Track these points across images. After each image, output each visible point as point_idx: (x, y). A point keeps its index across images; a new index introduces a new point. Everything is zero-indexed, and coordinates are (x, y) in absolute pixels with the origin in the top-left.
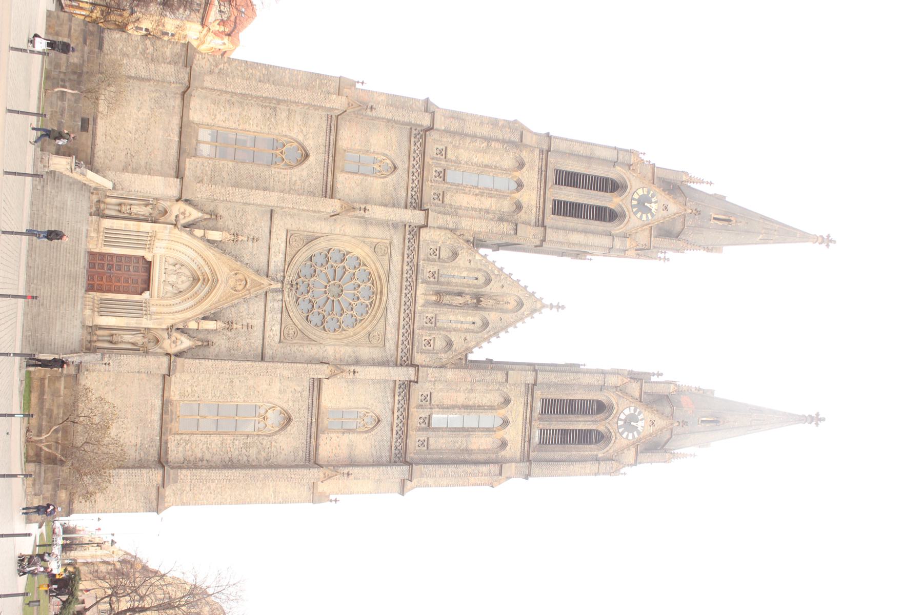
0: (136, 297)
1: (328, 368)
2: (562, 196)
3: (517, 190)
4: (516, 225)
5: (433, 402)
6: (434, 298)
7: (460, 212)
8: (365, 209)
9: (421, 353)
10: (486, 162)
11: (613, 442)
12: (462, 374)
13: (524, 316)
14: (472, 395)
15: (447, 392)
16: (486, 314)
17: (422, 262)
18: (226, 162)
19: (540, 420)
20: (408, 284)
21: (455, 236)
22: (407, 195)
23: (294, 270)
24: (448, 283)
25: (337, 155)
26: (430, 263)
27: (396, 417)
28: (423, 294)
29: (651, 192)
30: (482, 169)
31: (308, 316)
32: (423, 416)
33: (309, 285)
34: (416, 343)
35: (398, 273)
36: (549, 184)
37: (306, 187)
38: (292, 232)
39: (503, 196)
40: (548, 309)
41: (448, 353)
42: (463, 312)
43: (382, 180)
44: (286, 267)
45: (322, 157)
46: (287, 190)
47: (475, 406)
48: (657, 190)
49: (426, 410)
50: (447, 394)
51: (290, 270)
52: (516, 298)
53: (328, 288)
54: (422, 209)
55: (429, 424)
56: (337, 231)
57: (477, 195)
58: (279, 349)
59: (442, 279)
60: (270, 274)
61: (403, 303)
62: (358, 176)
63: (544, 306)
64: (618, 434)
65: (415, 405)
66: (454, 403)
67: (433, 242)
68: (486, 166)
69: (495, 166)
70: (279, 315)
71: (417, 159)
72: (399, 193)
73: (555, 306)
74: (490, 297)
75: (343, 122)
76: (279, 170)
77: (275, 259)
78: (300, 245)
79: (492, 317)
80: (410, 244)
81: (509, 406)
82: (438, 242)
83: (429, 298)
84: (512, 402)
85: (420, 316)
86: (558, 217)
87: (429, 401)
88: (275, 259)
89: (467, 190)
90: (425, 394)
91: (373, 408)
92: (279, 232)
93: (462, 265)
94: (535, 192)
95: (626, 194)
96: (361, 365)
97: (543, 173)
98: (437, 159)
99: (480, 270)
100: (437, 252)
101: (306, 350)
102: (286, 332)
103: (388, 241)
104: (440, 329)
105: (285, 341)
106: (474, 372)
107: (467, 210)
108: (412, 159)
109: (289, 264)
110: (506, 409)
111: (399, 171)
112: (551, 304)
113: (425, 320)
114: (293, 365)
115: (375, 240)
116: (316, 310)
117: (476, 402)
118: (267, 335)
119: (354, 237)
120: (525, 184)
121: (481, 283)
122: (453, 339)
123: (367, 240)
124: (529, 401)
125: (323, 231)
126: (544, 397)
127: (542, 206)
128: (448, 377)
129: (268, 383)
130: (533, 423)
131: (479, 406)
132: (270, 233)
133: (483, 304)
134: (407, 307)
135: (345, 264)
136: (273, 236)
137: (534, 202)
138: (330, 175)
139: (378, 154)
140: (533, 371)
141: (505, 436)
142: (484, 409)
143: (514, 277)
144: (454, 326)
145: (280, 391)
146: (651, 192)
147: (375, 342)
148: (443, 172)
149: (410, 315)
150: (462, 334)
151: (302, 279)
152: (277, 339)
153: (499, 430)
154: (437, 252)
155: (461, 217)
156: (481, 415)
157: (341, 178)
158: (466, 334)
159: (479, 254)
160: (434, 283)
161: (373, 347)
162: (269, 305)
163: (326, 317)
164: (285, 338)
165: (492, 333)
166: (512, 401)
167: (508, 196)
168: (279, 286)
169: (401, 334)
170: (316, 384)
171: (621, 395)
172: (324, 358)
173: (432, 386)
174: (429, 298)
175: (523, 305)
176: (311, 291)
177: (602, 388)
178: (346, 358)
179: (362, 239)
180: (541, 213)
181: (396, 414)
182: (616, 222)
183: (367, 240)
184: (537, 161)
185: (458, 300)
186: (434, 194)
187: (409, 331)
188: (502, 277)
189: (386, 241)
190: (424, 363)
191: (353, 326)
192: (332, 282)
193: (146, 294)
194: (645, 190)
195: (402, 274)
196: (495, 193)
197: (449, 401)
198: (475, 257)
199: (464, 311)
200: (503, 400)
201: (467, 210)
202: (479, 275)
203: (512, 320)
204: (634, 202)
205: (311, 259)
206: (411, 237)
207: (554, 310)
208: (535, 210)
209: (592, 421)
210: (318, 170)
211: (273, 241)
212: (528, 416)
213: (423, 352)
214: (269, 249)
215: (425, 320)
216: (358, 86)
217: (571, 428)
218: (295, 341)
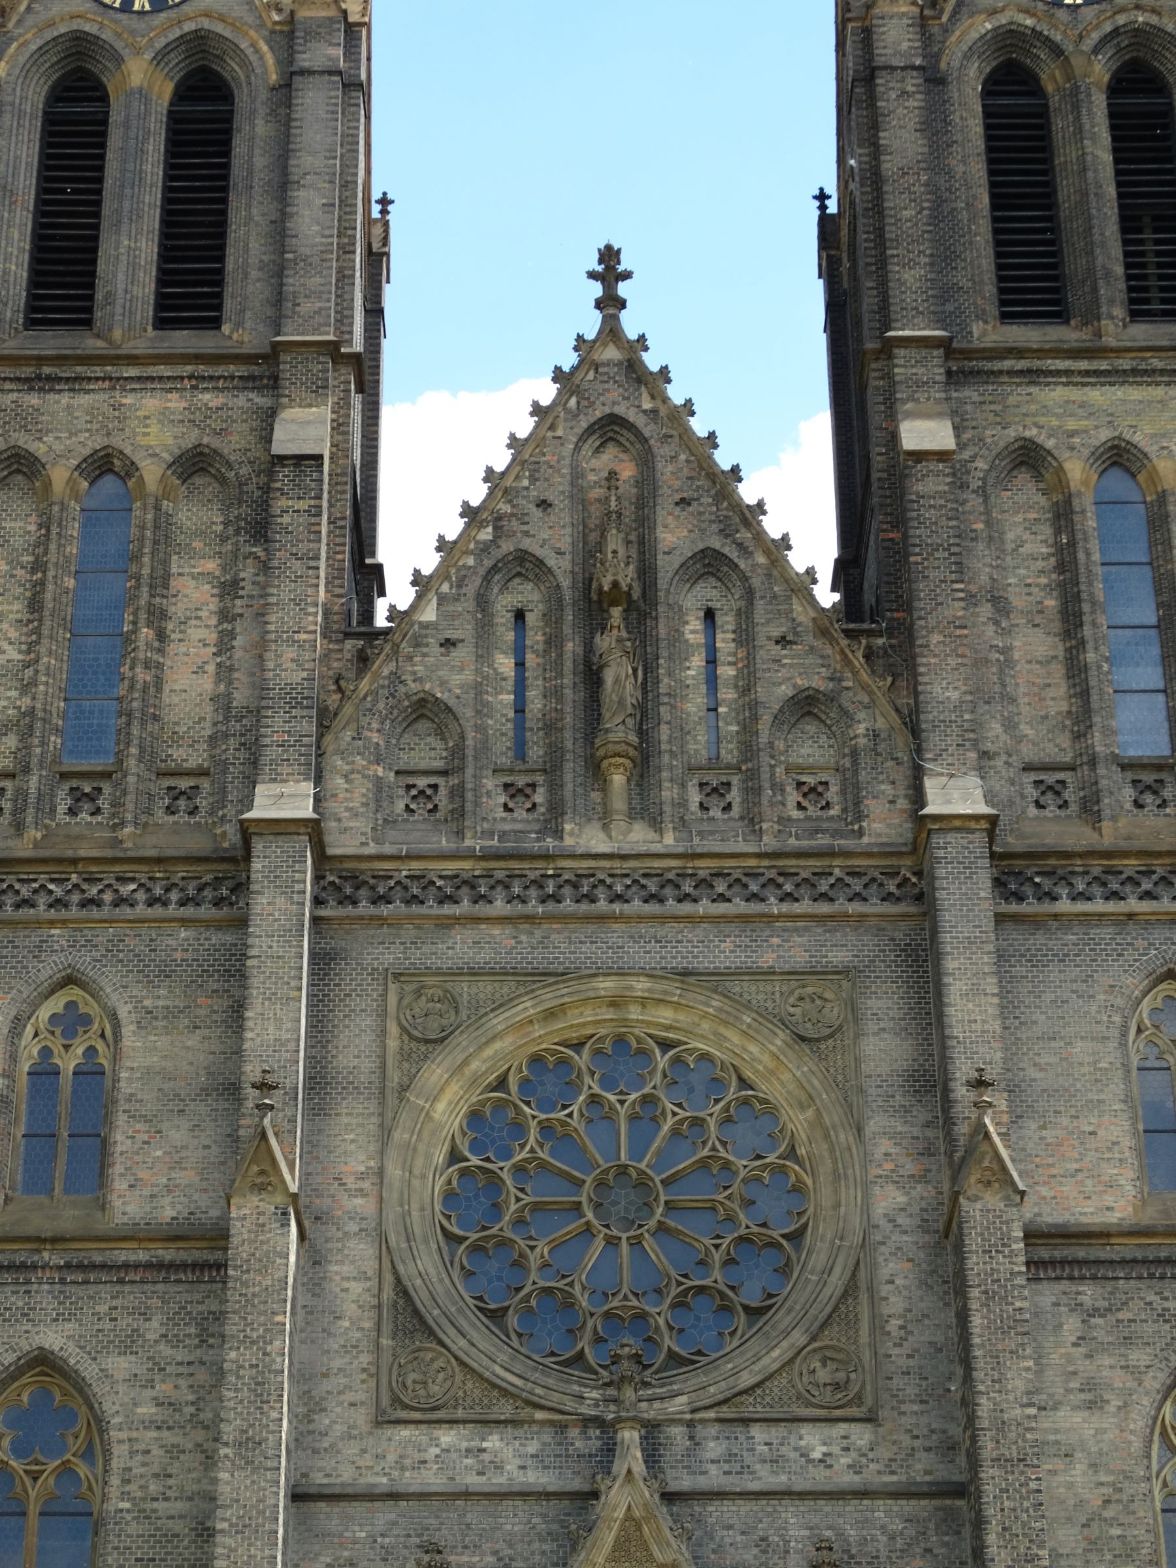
1: (976, 1198)
2: (137, 291)
3: (129, 475)
4: (282, 459)
5: (1067, 758)
6: (618, 780)
7: (240, 697)
8: (264, 1087)
9: (859, 817)
10: (16, 607)
11: (1154, 20)
12: (936, 638)
13: (663, 411)
14: (1018, 601)
15: (1013, 700)
16: (666, 566)
17: (468, 843)
19: (1092, 316)
20: (567, 891)
21: (348, 710)
22: (184, 922)
23: (551, 1382)
24: (551, 726)
25: (30, 1231)
26: (469, 807)
27: (1146, 906)
28: (606, 827)
30: (48, 623)
31: (746, 1308)
32: (1128, 793)
33: (608, 1315)
34: (822, 841)
35: (523, 938)
36: (92, 344)
37: (181, 1355)
38: (385, 1401)
39: (156, 527)
40: (624, 315)
41: (846, 704)
42: (670, 658)
43: (128, 1030)
44: (539, 1415)
45: (44, 1297)
46: (199, 1435)
47: (1062, 586)
49: (1104, 783)
50: (1023, 700)
51: (556, 1397)
52: (587, 449)
53: (615, 1232)
54: (240, 853)
55: (1159, 767)
56: (364, 1205)
57: (162, 636)
58: (906, 1421)
59: (535, 752)
60: (577, 1484)
61: (653, 908)
62: (121, 1141)
63: (611, 330)
65: (1087, 830)
66: (1058, 671)
67: (378, 801)
68: (35, 605)
69: (33, 571)
70: (758, 1433)
71: (25, 892)
72: (178, 955)
76: (115, 1481)
78: (440, 1363)
80: (398, 894)
81: (1050, 444)
82: (378, 782)
83: (619, 802)
84: (1031, 433)
85: (700, 833)
86: (229, 305)
87: (1061, 776)
89: (142, 675)
90: (1032, 793)
91: (1120, 1002)
92: (391, 1458)
93: (468, 676)
94: (128, 400)
95: (107, 35)
96: (945, 1059)
97: (47, 370)
98: (19, 811)
99: (483, 603)
100: (422, 782)
101: (895, 1304)
102: (828, 1397)
103: (393, 987)
104: (748, 750)
105: (869, 1401)
106: (922, 589)
107: (231, 669)
108: (26, 912)
109: (529, 1403)
110: (1064, 455)
111: (84, 961)
112: (599, 304)
113: (715, 812)
114: (978, 1353)
115: (393, 1044)
116: (716, 1276)
117: (1044, 580)
118: (848, 1480)
119: (385, 1133)
120: (98, 442)
121: (536, 596)
122: (785, 691)
123: (395, 1078)
124: (1021, 365)
125: (370, 1266)
126: (993, 310)
127: (189, 369)
128: (954, 695)
129: (1059, 1464)
130: (1110, 341)
131: (1061, 568)
132: (393, 1496)
133: (627, 576)
134: (668, 891)
135: (504, 1169)
136: (411, 1481)
137: (176, 403)
138: (122, 1257)
139: (13, 1058)
140: (890, 357)
142: (1072, 544)
143: (501, 460)
144: (727, 694)
145: (1090, 1406)
147: (834, 1013)
148: (74, 783)
149: (702, 874)
150: (761, 654)
151: (584, 1343)
152: (861, 1435)
153: (1154, 477)
154: (422, 782)
155: (261, 688)
156: (1096, 557)
158: (761, 640)
159: (414, 607)
160: (555, 787)
161: (856, 1021)
162: (714, 1478)
163: (743, 1231)
164: (858, 1400)
165: (744, 535)
166: (1027, 434)
167: (157, 508)
168: (630, 1436)
169: (785, 908)
170: (1044, 1254)
172: (924, 1226)
173: (999, 762)
174: (619, 802)
176: (635, 1303)
178: (916, 1131)
179: (392, 1100)
180: (220, 370)
181: (1133, 904)
182: (232, 69)
183: (395, 1078)
185: (617, 681)
186: (170, 810)
187: (772, 874)
188: (506, 508)
189: (392, 999)
190: (903, 804)
191: (770, 1110)
192: (590, 1215)
195: (529, 919)
196: (146, 559)
197: (1051, 693)
198: (425, 626)
199: (664, 653)
200: (1023, 478)
201: (231, 669)
202: (503, 604)
203: (683, 457)
205: (496, 1316)
206: (363, 892)
207: (623, 289)
208: (207, 397)
209: (1076, 108)
210: (103, 1308)
211: (432, 1479)
212: (1083, 365)
213: (855, 811)
214: (467, 1495)
215: (715, 812)
217: (1111, 191)
218: (867, 1356)
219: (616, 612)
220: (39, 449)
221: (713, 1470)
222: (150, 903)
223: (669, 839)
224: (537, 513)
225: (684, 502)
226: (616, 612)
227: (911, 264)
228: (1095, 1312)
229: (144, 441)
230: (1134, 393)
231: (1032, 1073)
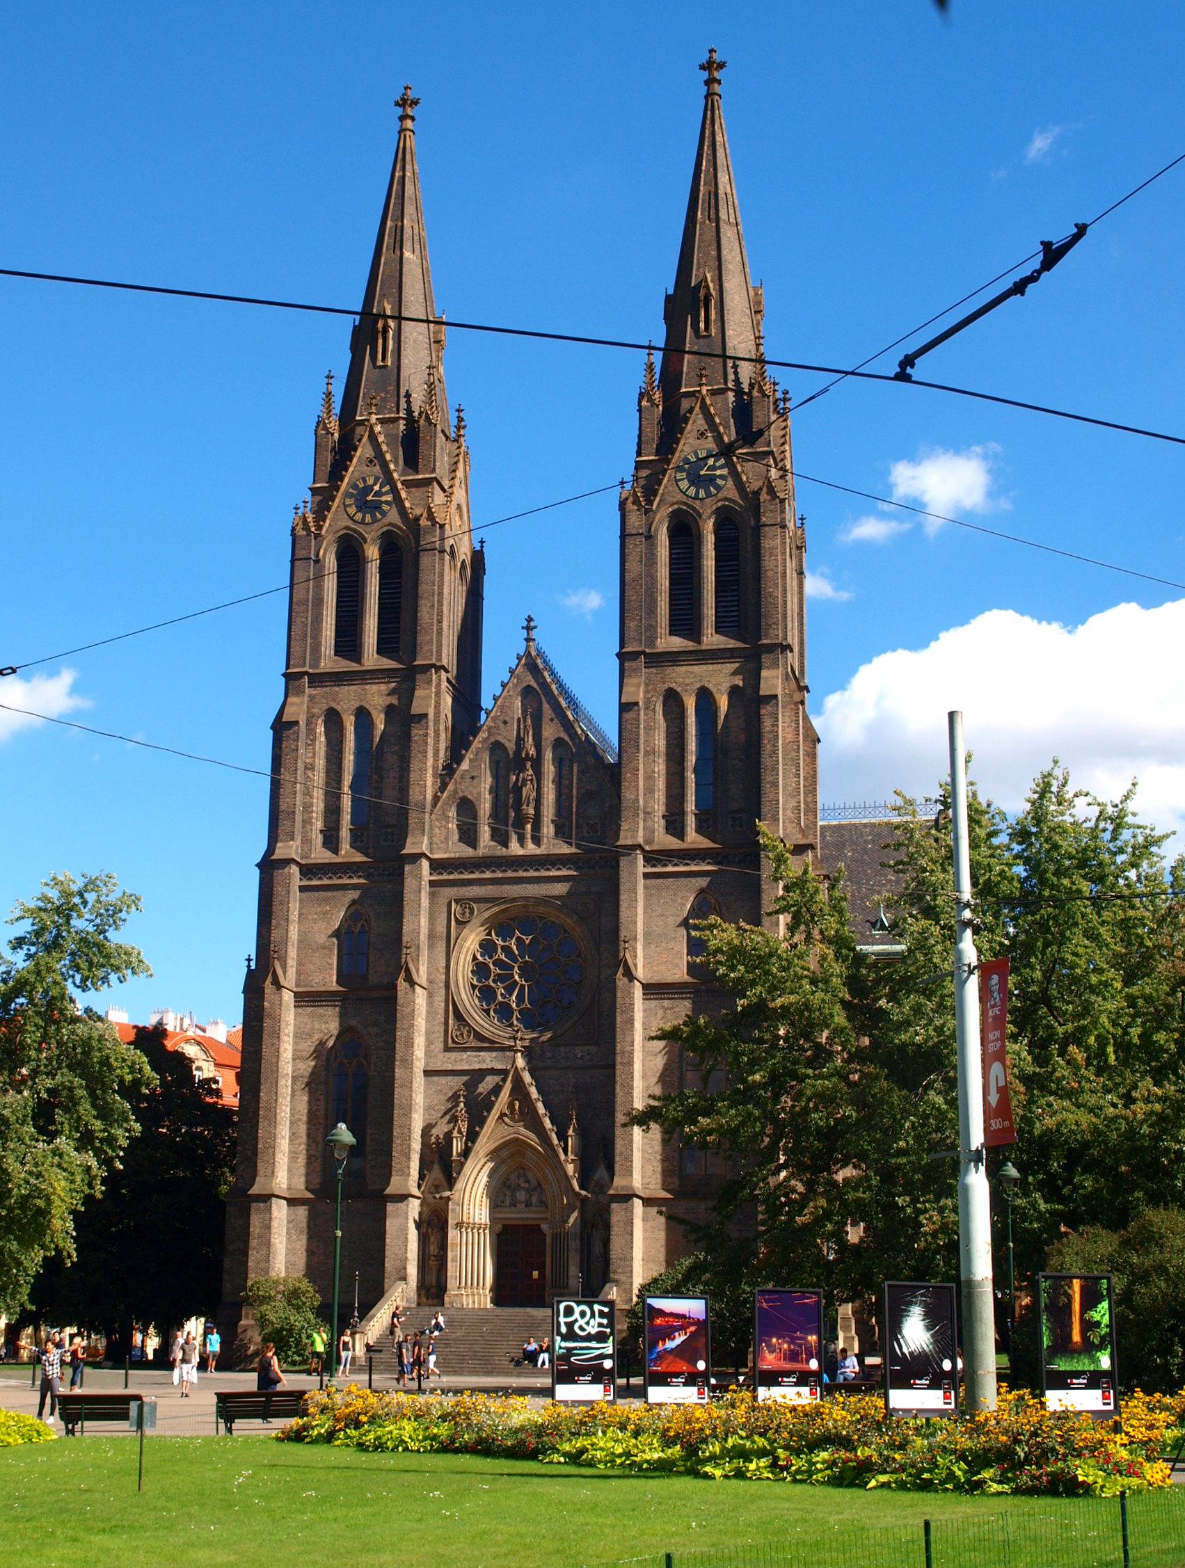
0: (549, 1240)
1: (620, 980)
12: (628, 775)
18: (368, 1138)
29: (351, 490)
36: (354, 666)
43: (373, 920)
48: (346, 480)
57: (381, 777)
64: (720, 495)
70: (562, 1049)
73: (528, 634)
74: (520, 741)
75: (303, 983)
76: (372, 1066)
77: (488, 1061)
79: (550, 731)
81: (679, 689)
84: (673, 685)
88: (488, 1061)
94: (367, 687)
115: (453, 923)
120: (357, 705)
128: (633, 797)
137: (383, 687)
141: (723, 690)
146: (351, 490)
152: (593, 1049)
157: (373, 979)
171: (658, 499)
175: (529, 687)
177: (650, 537)
184: (325, 689)
186: (385, 840)
193: (545, 1227)
194: (348, 502)
198: (466, 771)
204: (368, 518)
207: (534, 634)
216: (253, 967)
219: (529, 765)
220: (338, 708)
221: (548, 1061)
222: (378, 876)
223: (543, 847)
224: (503, 725)
225: (552, 720)
226: (529, 765)
227: (633, 620)
228: (668, 1009)
229: (372, 703)
230: (711, 667)
231: (655, 928)
